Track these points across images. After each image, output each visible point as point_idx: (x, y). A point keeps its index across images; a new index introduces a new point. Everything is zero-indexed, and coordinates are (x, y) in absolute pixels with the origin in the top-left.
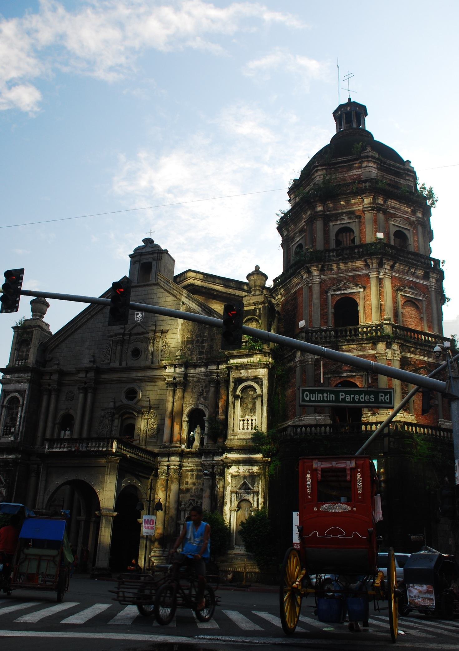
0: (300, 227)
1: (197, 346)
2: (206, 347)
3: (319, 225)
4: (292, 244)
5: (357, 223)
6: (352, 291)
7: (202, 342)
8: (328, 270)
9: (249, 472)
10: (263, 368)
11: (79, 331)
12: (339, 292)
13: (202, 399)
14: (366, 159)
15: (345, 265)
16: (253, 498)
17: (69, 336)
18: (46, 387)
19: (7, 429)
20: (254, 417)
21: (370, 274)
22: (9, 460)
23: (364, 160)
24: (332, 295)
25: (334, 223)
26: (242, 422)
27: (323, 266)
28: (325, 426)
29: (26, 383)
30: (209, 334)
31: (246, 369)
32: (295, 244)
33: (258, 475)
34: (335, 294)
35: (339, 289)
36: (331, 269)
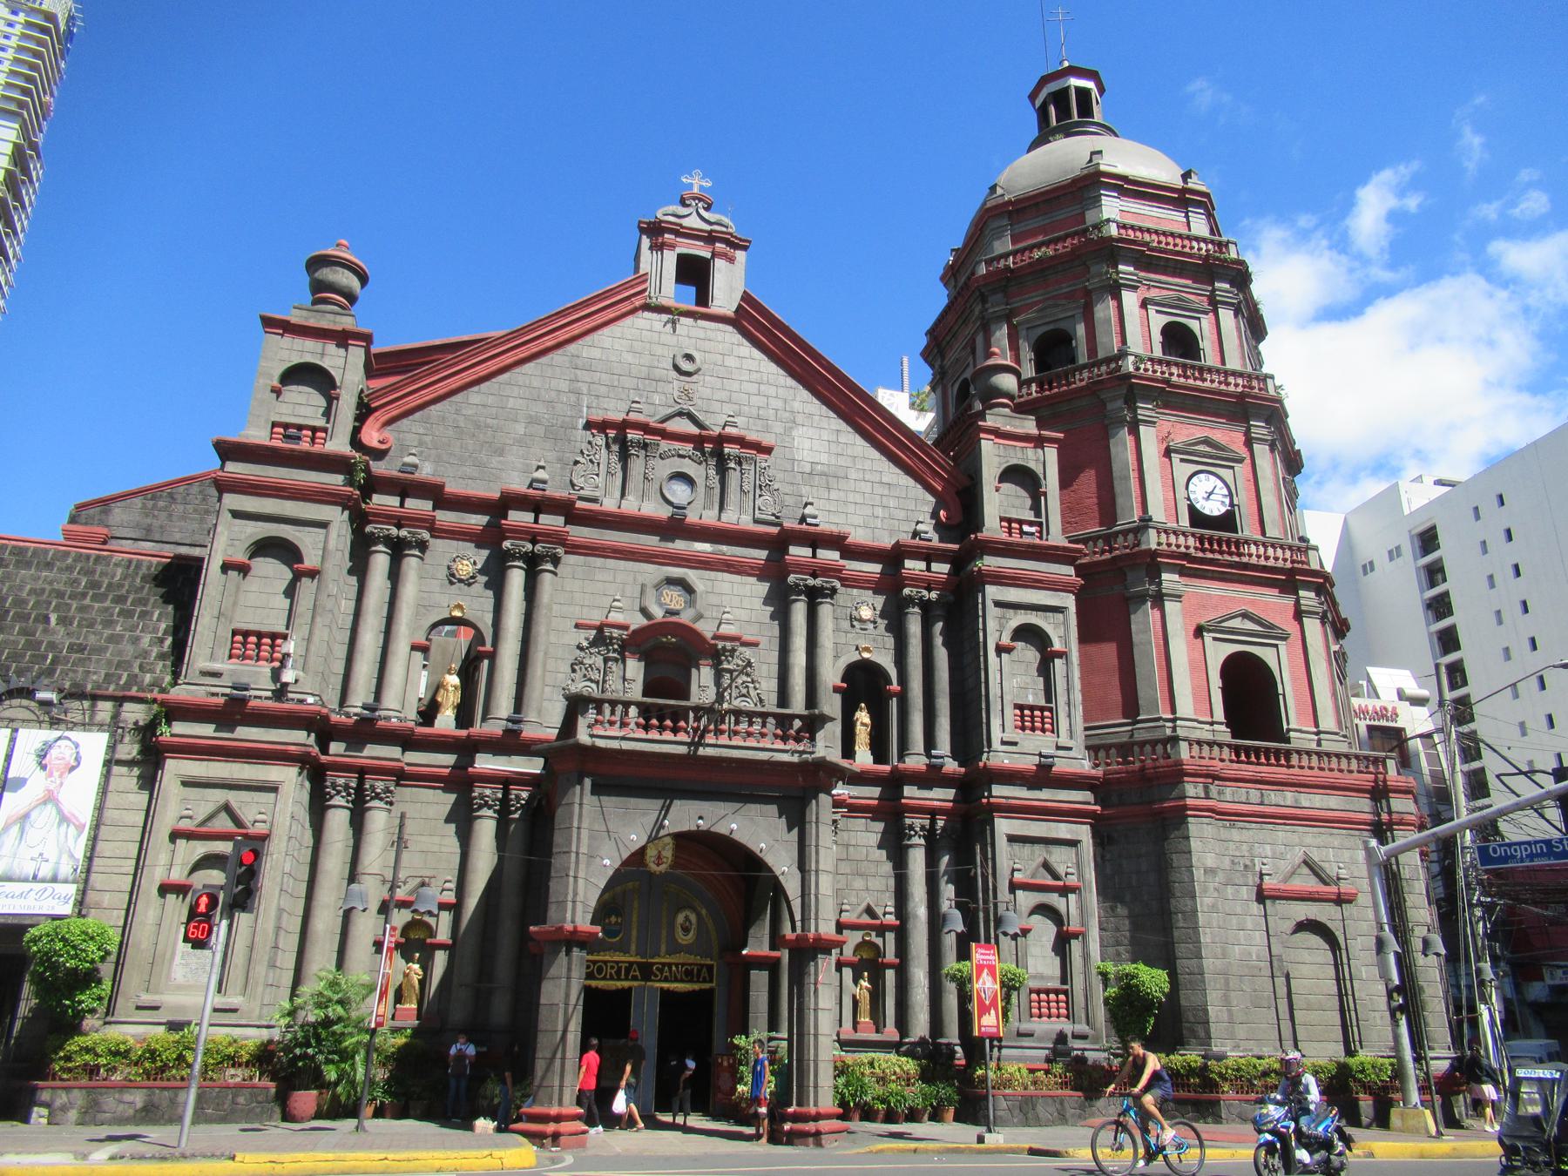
18: (388, 530)
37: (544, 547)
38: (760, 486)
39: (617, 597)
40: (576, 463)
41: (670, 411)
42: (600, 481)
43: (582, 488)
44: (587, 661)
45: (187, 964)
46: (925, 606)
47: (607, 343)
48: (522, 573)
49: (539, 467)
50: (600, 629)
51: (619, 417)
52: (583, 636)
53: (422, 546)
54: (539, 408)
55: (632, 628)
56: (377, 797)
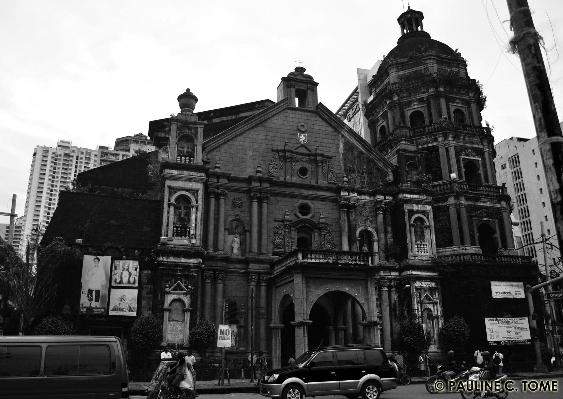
0: (418, 98)
1: (359, 176)
2: (367, 179)
3: (443, 102)
4: (408, 109)
5: (466, 108)
6: (474, 158)
7: (363, 174)
8: (457, 138)
9: (429, 287)
10: (429, 205)
11: (239, 138)
12: (467, 157)
13: (369, 223)
14: (462, 63)
15: (468, 138)
16: (434, 308)
17: (229, 141)
18: (215, 190)
19: (177, 230)
20: (423, 243)
21: (485, 149)
22: (191, 264)
23: (461, 63)
24: (462, 158)
25: (452, 104)
26: (416, 246)
27: (455, 136)
28: (478, 255)
29: (199, 182)
30: (367, 168)
31: (417, 204)
32: (411, 109)
33: (435, 289)
34: (464, 158)
35: (467, 155)
36: (459, 139)
37: (264, 195)
38: (329, 171)
39: (287, 211)
40: (271, 164)
41: (298, 145)
42: (278, 170)
43: (273, 173)
44: (279, 232)
45: (171, 334)
46: (385, 212)
47: (276, 122)
48: (257, 203)
49: (258, 167)
50: (283, 221)
51: (281, 148)
52: (277, 224)
53: (225, 195)
54: (256, 145)
55: (294, 221)
56: (220, 279)
